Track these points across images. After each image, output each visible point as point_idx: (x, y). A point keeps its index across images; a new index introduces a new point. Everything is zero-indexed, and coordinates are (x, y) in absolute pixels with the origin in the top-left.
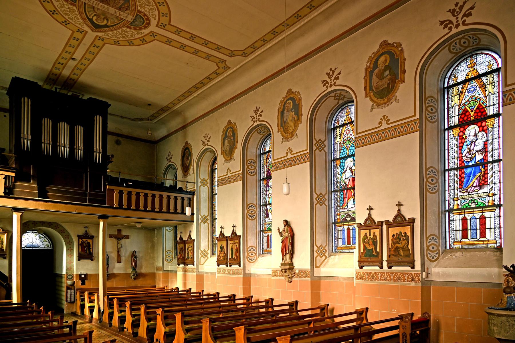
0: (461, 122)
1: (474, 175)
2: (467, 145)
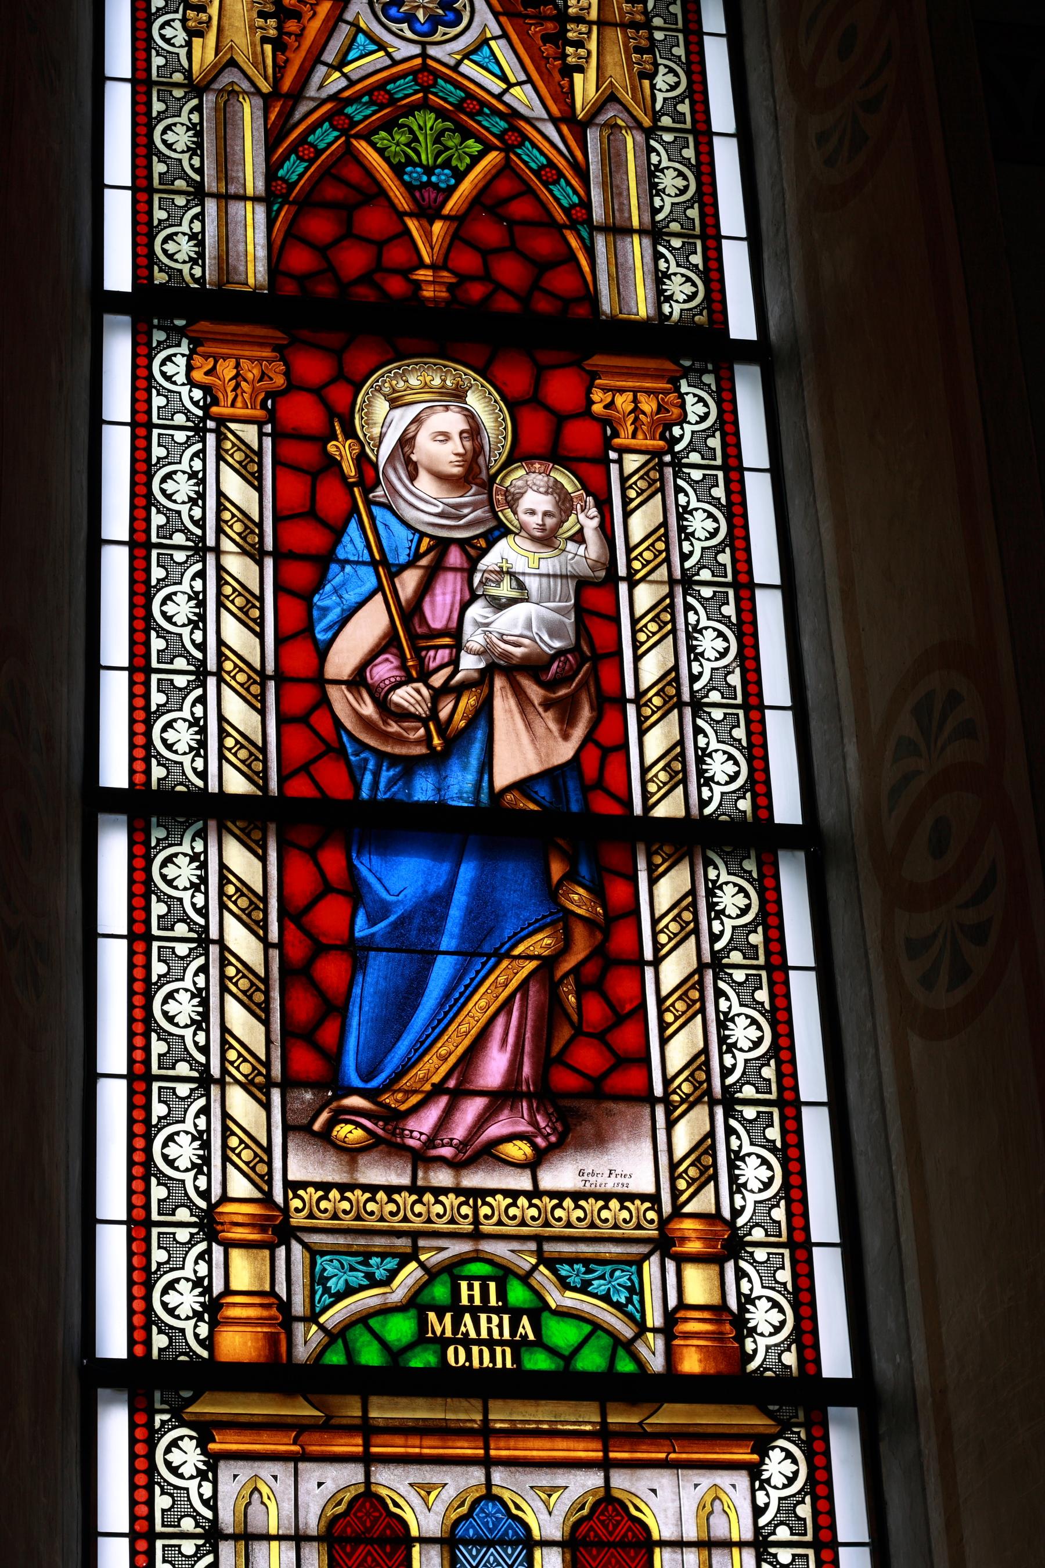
0: (302, 279)
1: (482, 950)
2: (387, 569)
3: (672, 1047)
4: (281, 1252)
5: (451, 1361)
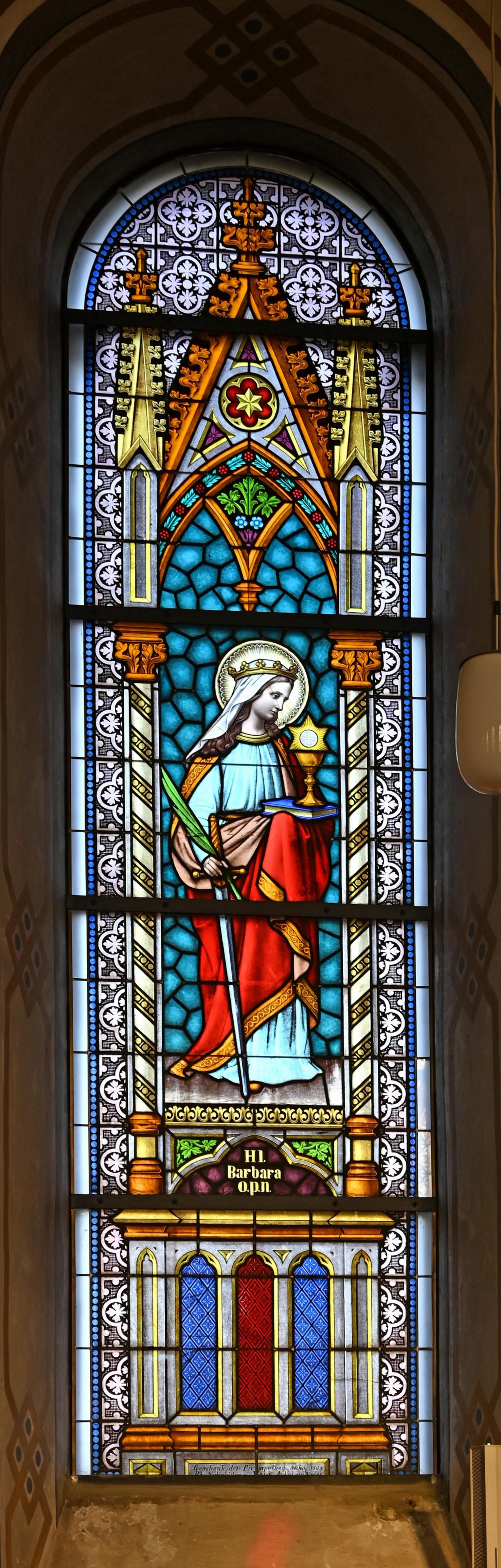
3: (355, 1030)
4: (161, 1139)
5: (240, 1190)
